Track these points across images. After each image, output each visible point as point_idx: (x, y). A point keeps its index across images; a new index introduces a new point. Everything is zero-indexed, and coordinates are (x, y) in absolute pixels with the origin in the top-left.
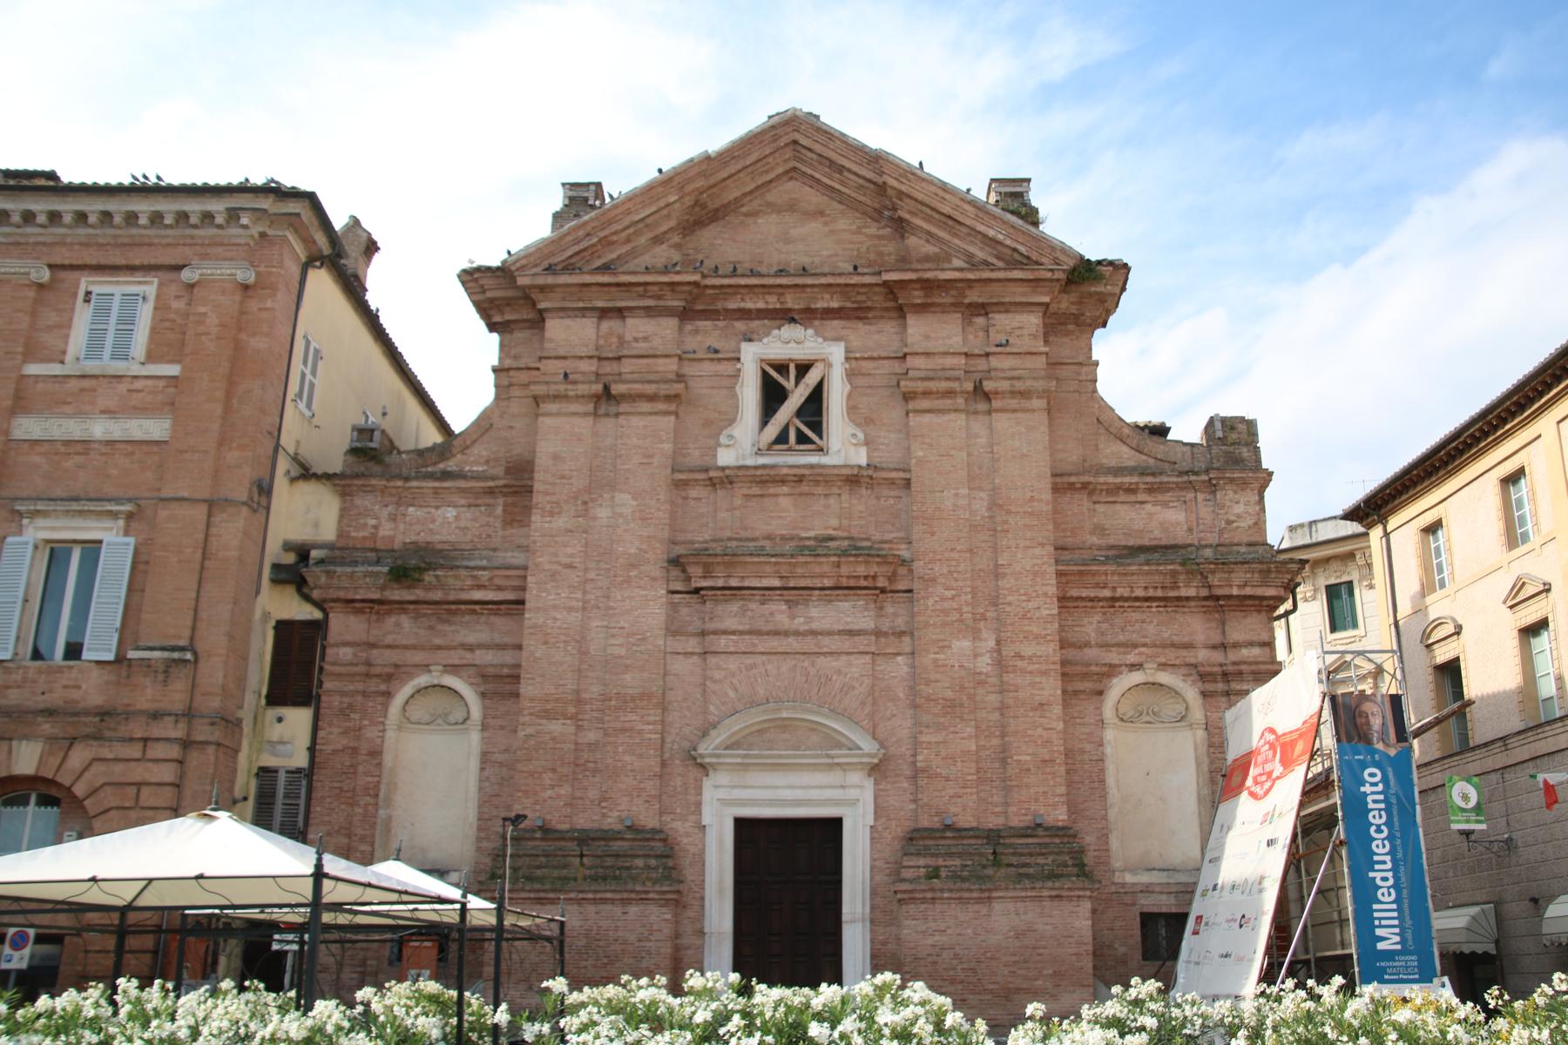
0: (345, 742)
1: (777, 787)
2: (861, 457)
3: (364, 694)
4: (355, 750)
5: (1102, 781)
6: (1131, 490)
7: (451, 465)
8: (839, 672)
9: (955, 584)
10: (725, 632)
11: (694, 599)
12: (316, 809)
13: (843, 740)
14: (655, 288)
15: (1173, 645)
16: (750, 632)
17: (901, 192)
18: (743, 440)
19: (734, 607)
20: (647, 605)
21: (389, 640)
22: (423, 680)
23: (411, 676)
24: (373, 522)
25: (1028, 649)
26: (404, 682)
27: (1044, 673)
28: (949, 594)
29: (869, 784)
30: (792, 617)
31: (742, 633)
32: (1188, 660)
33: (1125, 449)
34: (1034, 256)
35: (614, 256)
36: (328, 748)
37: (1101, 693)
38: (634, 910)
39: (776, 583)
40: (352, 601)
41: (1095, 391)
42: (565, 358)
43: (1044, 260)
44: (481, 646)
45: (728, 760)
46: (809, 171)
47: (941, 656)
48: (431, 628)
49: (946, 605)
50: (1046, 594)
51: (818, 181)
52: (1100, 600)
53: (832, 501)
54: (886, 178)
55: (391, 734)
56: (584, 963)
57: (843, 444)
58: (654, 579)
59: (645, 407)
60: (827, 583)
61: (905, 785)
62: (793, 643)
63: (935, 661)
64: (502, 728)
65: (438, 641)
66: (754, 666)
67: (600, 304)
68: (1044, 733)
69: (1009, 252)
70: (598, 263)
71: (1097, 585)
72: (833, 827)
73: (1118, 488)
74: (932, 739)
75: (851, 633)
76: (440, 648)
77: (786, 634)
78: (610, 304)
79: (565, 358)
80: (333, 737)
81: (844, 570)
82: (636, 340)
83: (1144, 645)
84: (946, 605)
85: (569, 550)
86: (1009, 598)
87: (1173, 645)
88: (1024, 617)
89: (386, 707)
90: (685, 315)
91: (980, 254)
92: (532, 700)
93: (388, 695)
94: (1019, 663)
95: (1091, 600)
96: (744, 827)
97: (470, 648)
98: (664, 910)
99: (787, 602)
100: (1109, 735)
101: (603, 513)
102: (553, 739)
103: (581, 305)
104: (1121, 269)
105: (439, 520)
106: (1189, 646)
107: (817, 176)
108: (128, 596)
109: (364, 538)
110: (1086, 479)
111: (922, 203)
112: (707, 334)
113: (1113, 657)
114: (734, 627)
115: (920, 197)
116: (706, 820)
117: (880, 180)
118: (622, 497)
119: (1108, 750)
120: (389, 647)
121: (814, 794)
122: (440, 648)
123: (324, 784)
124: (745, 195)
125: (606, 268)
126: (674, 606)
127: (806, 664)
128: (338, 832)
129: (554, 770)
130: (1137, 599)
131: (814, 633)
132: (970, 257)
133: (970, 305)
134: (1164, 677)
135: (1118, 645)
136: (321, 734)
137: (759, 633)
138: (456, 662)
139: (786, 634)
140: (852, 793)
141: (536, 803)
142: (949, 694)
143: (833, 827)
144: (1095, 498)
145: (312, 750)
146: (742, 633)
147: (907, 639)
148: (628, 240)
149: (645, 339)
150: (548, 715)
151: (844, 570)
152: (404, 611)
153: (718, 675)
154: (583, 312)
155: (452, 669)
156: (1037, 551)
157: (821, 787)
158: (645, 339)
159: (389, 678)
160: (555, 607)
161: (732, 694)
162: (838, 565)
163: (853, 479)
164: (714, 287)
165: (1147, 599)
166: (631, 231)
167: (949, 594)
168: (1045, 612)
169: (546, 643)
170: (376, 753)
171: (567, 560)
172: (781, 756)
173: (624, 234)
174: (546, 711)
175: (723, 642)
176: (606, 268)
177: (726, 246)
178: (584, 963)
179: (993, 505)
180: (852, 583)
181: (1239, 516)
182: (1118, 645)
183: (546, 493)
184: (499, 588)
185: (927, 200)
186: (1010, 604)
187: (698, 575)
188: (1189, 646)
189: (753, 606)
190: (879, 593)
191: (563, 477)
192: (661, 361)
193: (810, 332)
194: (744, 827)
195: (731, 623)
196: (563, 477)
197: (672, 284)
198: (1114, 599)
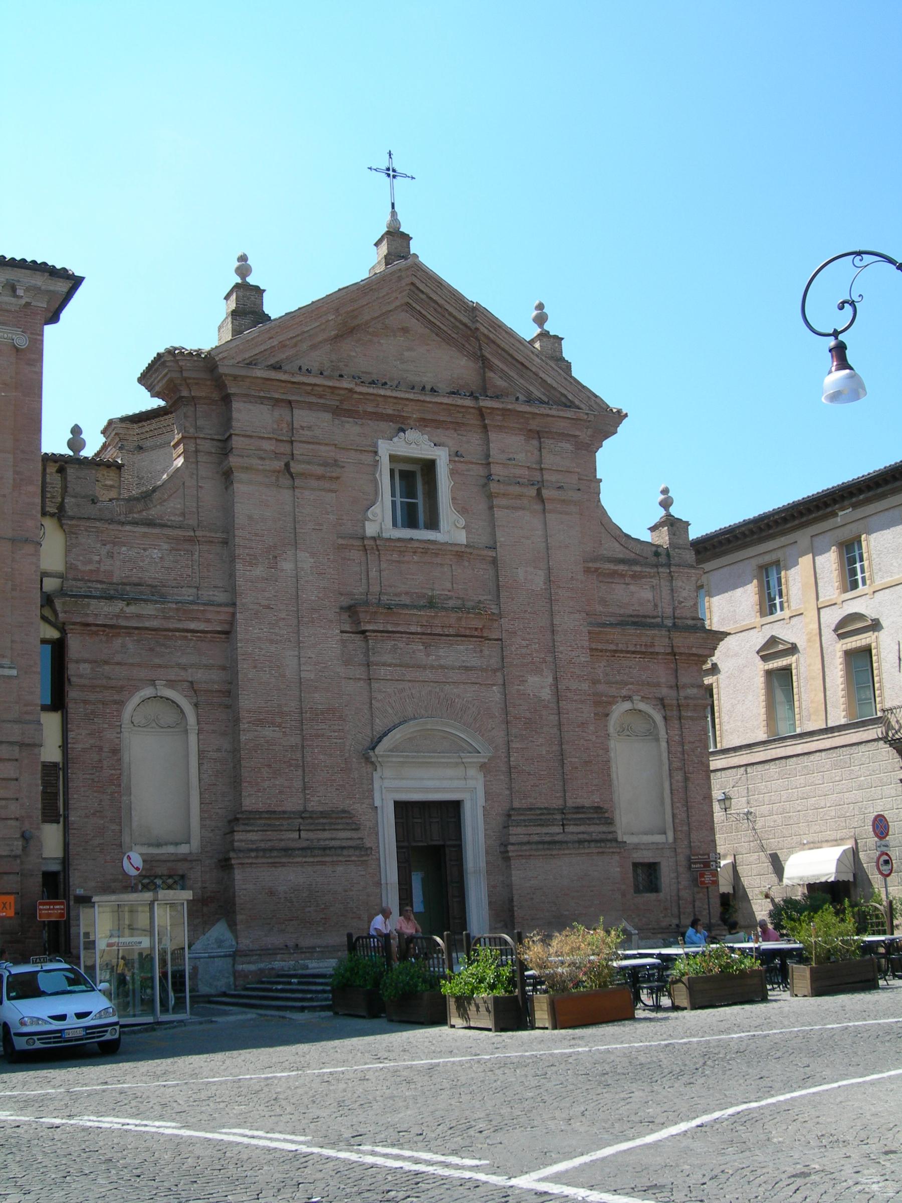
0: (92, 741)
1: (423, 779)
2: (461, 537)
3: (104, 703)
4: (101, 749)
5: (609, 775)
6: (622, 576)
7: (154, 512)
8: (459, 696)
9: (528, 636)
10: (384, 665)
11: (358, 637)
12: (74, 796)
13: (464, 745)
14: (320, 389)
15: (648, 684)
16: (400, 666)
17: (488, 338)
18: (381, 519)
19: (389, 644)
20: (327, 642)
21: (118, 658)
22: (148, 692)
23: (137, 689)
24: (97, 558)
25: (574, 685)
26: (132, 694)
27: (582, 702)
28: (524, 643)
29: (481, 777)
30: (428, 655)
31: (396, 665)
32: (657, 695)
33: (617, 545)
34: (577, 402)
35: (284, 356)
36: (79, 746)
37: (607, 715)
38: (340, 869)
39: (419, 630)
40: (88, 625)
41: (599, 501)
42: (250, 437)
43: (582, 406)
44: (192, 666)
45: (394, 759)
46: (418, 308)
47: (522, 688)
48: (151, 650)
49: (524, 651)
50: (582, 647)
51: (424, 316)
52: (606, 651)
53: (446, 569)
54: (478, 325)
55: (125, 734)
56: (308, 909)
57: (452, 528)
58: (331, 621)
59: (314, 483)
60: (452, 631)
61: (502, 777)
62: (429, 675)
63: (518, 691)
64: (214, 732)
65: (157, 661)
66: (403, 690)
67: (277, 396)
68: (585, 743)
69: (559, 396)
70: (272, 361)
71: (607, 642)
72: (455, 807)
73: (613, 574)
74: (518, 745)
75: (467, 668)
76: (160, 666)
77: (424, 667)
78: (284, 397)
79: (250, 437)
80: (81, 738)
81: (463, 623)
82: (302, 428)
83: (632, 684)
84: (524, 651)
85: (267, 594)
86: (561, 648)
87: (648, 684)
88: (570, 662)
89: (120, 712)
90: (338, 412)
91: (537, 393)
92: (249, 711)
93: (121, 703)
94: (569, 694)
95: (601, 651)
96: (401, 807)
97: (184, 668)
98: (360, 868)
99: (423, 644)
100: (612, 744)
101: (287, 566)
102: (267, 742)
103: (262, 394)
104: (620, 416)
105: (147, 560)
106: (658, 685)
107: (424, 312)
108: (713, 702)
109: (91, 571)
110: (598, 565)
111: (503, 350)
112: (351, 430)
113: (613, 691)
114: (389, 661)
115: (503, 345)
116: (377, 803)
117: (473, 326)
118: (302, 555)
119: (612, 755)
120: (118, 664)
121: (446, 784)
122: (160, 666)
123: (78, 778)
124: (373, 319)
125: (277, 367)
126: (343, 642)
127: (438, 690)
128: (94, 814)
129: (269, 766)
130: (628, 652)
131: (442, 667)
132: (529, 393)
133: (530, 430)
134: (642, 706)
135: (616, 683)
136: (71, 735)
137: (407, 666)
138: (173, 678)
139: (424, 667)
140: (471, 783)
141: (259, 791)
142: (528, 715)
143: (455, 807)
144: (600, 579)
145: (64, 747)
146: (396, 665)
147: (499, 674)
148: (295, 345)
149: (309, 428)
150: (260, 723)
151: (463, 623)
152: (129, 634)
153: (380, 697)
154: (262, 400)
155: (171, 684)
156: (577, 616)
157: (451, 779)
158: (309, 428)
159: (121, 689)
160: (259, 639)
161: (390, 711)
162: (460, 619)
163: (460, 554)
164: (361, 393)
165: (634, 652)
166: (299, 338)
167: (524, 643)
168: (583, 659)
169: (255, 667)
170: (116, 751)
171: (265, 603)
172: (424, 757)
173: (294, 340)
174: (259, 720)
175: (383, 672)
176: (277, 367)
177: (363, 358)
178: (308, 909)
179: (549, 580)
180: (468, 632)
181: (685, 598)
182: (616, 683)
183: (245, 547)
184: (208, 621)
185: (507, 348)
186: (562, 653)
187: (360, 617)
188: (658, 685)
189: (401, 645)
190: (478, 636)
191: (256, 535)
192: (323, 448)
193: (426, 437)
194: (401, 807)
195: (387, 658)
196: (256, 535)
197: (333, 388)
198: (616, 651)
